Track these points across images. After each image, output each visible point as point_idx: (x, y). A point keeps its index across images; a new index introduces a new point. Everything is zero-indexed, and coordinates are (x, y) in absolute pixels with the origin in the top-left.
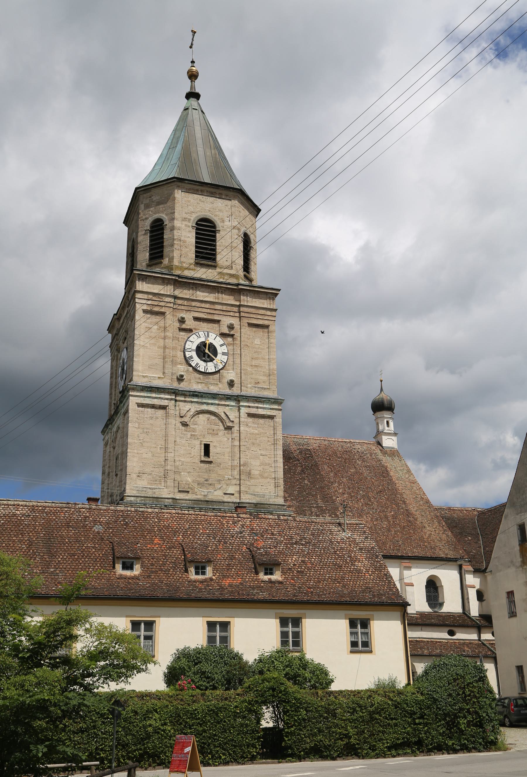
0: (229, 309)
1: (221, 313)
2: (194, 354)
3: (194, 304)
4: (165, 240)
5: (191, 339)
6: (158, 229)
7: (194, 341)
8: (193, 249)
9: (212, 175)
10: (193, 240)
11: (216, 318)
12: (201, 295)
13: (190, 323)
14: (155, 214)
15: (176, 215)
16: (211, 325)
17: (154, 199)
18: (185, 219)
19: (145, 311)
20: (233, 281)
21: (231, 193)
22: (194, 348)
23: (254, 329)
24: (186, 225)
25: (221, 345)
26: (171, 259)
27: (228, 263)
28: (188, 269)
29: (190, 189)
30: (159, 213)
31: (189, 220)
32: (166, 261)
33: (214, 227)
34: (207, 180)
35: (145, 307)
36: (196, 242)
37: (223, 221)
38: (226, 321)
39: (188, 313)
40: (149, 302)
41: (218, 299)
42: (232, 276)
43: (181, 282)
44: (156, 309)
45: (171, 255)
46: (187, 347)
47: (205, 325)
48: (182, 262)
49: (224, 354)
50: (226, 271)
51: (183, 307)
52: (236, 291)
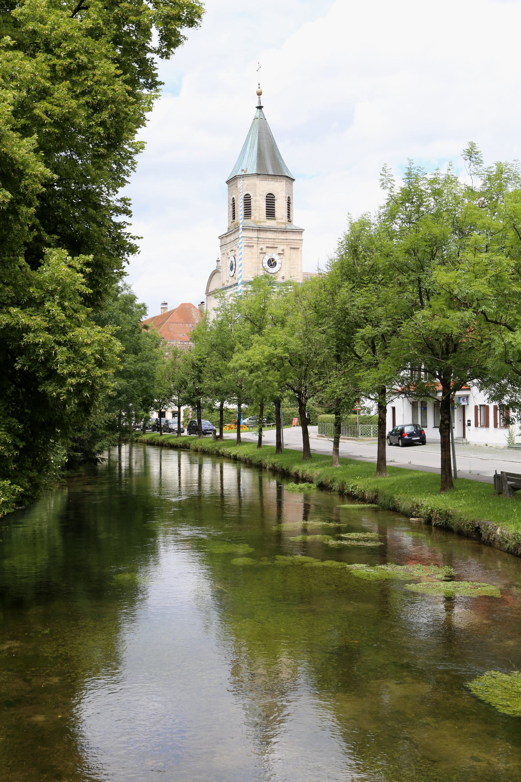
0: (281, 241)
2: (267, 265)
3: (266, 240)
6: (247, 199)
8: (265, 210)
9: (274, 171)
11: (276, 246)
12: (270, 235)
15: (257, 194)
16: (273, 250)
18: (261, 195)
19: (245, 246)
20: (283, 226)
21: (282, 178)
22: (267, 262)
26: (255, 217)
32: (252, 218)
33: (274, 197)
35: (245, 244)
37: (278, 194)
38: (281, 247)
40: (247, 241)
42: (282, 223)
43: (260, 230)
48: (260, 219)
49: (279, 263)
50: (279, 221)
52: (285, 231)
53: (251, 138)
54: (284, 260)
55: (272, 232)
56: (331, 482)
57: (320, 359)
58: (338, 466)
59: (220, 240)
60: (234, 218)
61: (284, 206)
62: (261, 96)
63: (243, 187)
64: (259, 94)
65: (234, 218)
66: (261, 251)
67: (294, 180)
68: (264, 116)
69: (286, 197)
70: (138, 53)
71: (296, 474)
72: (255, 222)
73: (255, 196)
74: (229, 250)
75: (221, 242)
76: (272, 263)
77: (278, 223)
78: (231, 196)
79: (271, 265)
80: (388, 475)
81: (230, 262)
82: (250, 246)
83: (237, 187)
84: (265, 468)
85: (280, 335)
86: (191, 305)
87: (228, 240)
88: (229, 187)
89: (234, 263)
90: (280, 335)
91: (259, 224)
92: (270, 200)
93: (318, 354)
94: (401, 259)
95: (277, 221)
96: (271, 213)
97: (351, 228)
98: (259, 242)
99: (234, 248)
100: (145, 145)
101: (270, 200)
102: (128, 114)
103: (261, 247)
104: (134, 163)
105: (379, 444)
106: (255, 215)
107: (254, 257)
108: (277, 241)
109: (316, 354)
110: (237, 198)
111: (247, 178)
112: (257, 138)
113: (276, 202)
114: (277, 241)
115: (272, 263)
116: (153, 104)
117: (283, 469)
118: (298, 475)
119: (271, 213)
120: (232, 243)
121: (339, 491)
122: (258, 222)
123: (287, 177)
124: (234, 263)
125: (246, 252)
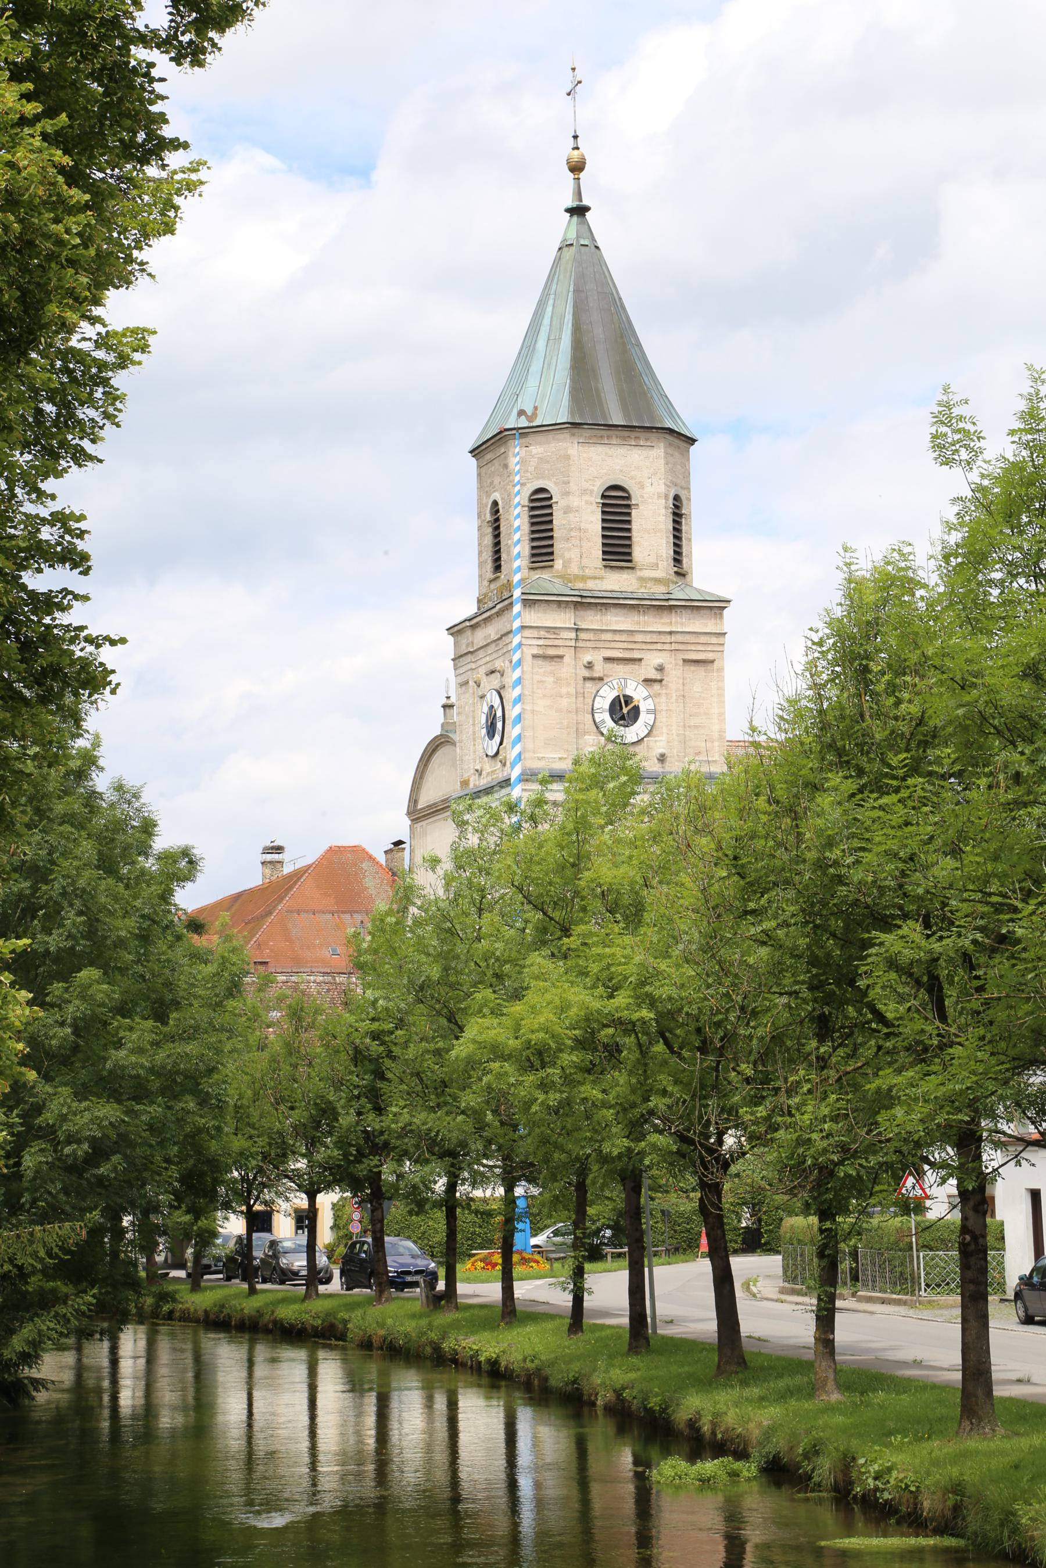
0: (655, 638)
1: (644, 646)
4: (555, 528)
5: (601, 693)
6: (541, 505)
7: (607, 695)
8: (600, 540)
10: (599, 525)
11: (636, 655)
13: (598, 670)
14: (538, 478)
15: (573, 487)
16: (629, 667)
17: (534, 451)
18: (584, 492)
19: (534, 656)
20: (659, 590)
21: (653, 436)
22: (607, 706)
23: (693, 668)
24: (587, 503)
25: (645, 699)
26: (567, 564)
27: (652, 559)
28: (595, 578)
29: (590, 438)
30: (543, 478)
31: (592, 491)
32: (558, 564)
33: (628, 498)
34: (617, 419)
35: (535, 651)
36: (603, 528)
37: (642, 487)
38: (653, 659)
39: (596, 652)
40: (541, 642)
41: (639, 623)
42: (657, 581)
43: (582, 603)
44: (551, 652)
45: (567, 555)
46: (596, 706)
47: (620, 669)
48: (583, 568)
49: (649, 711)
51: (588, 644)
52: (665, 607)
53: (549, 309)
54: (663, 699)
55: (625, 611)
56: (806, 1456)
57: (763, 1029)
58: (835, 1397)
59: (451, 638)
60: (498, 568)
61: (663, 526)
62: (582, 175)
63: (526, 466)
64: (577, 168)
65: (498, 568)
66: (587, 674)
67: (692, 441)
68: (594, 240)
69: (666, 497)
70: (95, 47)
71: (693, 1425)
72: (565, 578)
73: (567, 494)
74: (482, 671)
75: (456, 644)
76: (625, 710)
77: (642, 580)
78: (488, 495)
79: (623, 718)
80: (1001, 1431)
81: (486, 709)
82: (552, 658)
83: (506, 466)
84: (593, 1404)
85: (628, 951)
86: (359, 853)
87: (480, 637)
88: (479, 467)
89: (499, 714)
90: (628, 951)
91: (580, 585)
92: (616, 506)
93: (755, 1014)
94: (1007, 699)
95: (639, 573)
96: (617, 549)
97: (849, 596)
98: (580, 644)
99: (498, 664)
100: (151, 340)
101: (616, 506)
102: (60, 243)
103: (588, 658)
104: (113, 397)
105: (964, 1321)
106: (567, 555)
107: (564, 690)
108: (639, 638)
109: (749, 1014)
110: (508, 502)
111: (539, 438)
112: (570, 309)
113: (634, 512)
114: (639, 638)
115: (624, 711)
116: (176, 208)
117: (649, 1411)
118: (698, 1430)
119: (617, 549)
120: (492, 649)
121: (836, 1488)
122: (577, 578)
123: (671, 431)
124: (499, 714)
125: (537, 677)
